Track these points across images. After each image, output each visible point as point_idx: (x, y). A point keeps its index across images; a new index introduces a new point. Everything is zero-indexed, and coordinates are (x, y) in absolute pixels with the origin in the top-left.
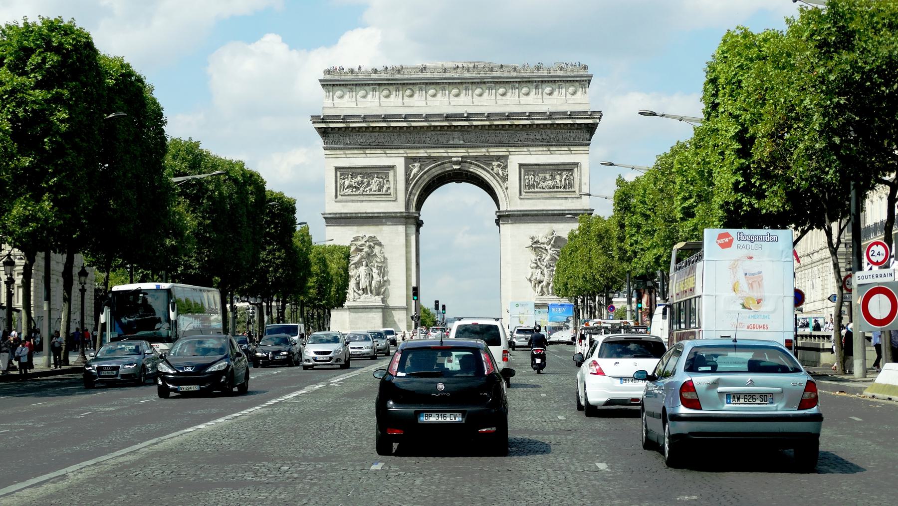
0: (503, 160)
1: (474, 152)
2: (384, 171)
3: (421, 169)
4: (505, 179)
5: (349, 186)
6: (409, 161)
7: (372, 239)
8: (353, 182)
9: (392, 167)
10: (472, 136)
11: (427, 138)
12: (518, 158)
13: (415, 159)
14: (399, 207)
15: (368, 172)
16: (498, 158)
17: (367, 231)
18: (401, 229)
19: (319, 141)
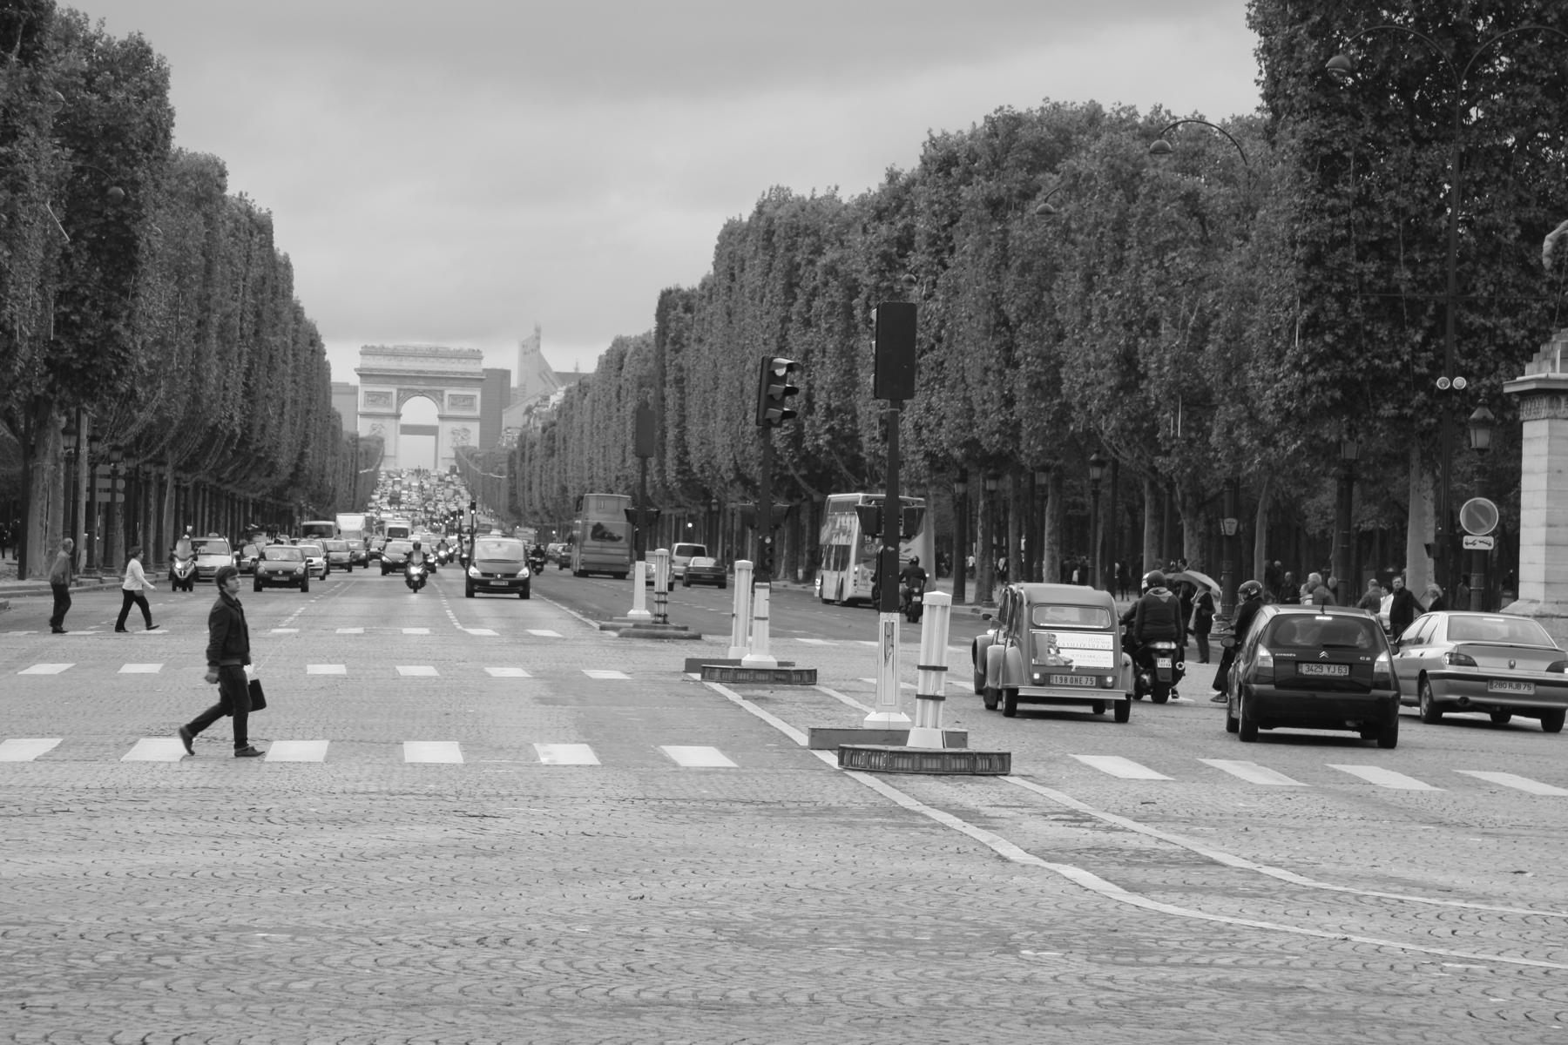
0: (442, 392)
2: (388, 395)
12: (448, 392)
14: (393, 411)
15: (380, 395)
17: (377, 422)
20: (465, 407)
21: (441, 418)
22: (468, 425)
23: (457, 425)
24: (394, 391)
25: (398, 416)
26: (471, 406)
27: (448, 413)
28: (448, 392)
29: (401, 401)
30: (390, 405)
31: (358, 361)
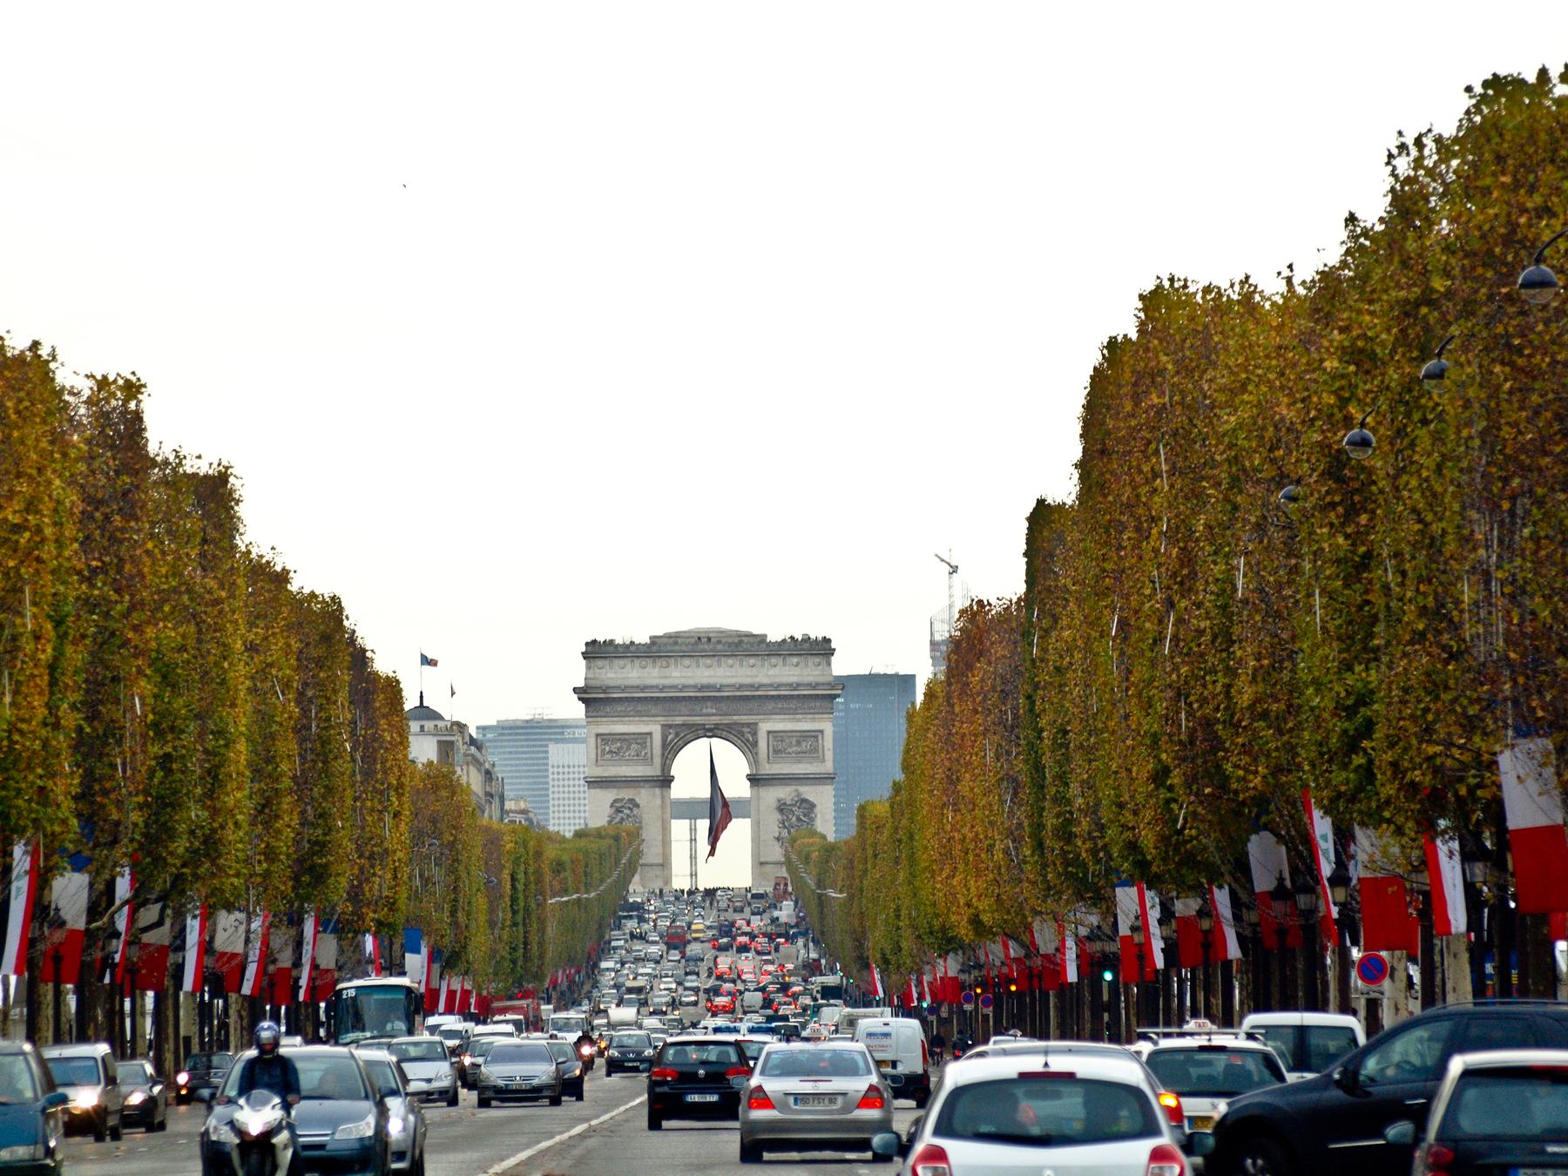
0: (753, 728)
1: (726, 720)
3: (677, 735)
4: (755, 744)
5: (611, 752)
6: (665, 727)
7: (631, 801)
8: (614, 747)
9: (650, 734)
10: (724, 707)
11: (683, 707)
13: (670, 726)
14: (654, 770)
15: (625, 738)
16: (748, 725)
17: (626, 794)
18: (657, 791)
19: (582, 706)
20: (800, 757)
21: (754, 780)
22: (808, 792)
23: (785, 792)
24: (656, 730)
25: (666, 781)
26: (814, 753)
27: (768, 769)
28: (765, 727)
29: (671, 750)
30: (648, 760)
31: (578, 673)
